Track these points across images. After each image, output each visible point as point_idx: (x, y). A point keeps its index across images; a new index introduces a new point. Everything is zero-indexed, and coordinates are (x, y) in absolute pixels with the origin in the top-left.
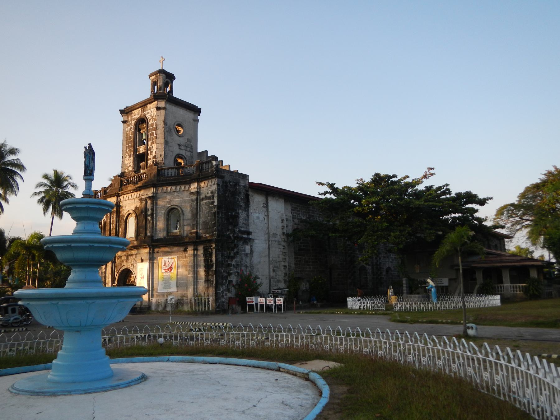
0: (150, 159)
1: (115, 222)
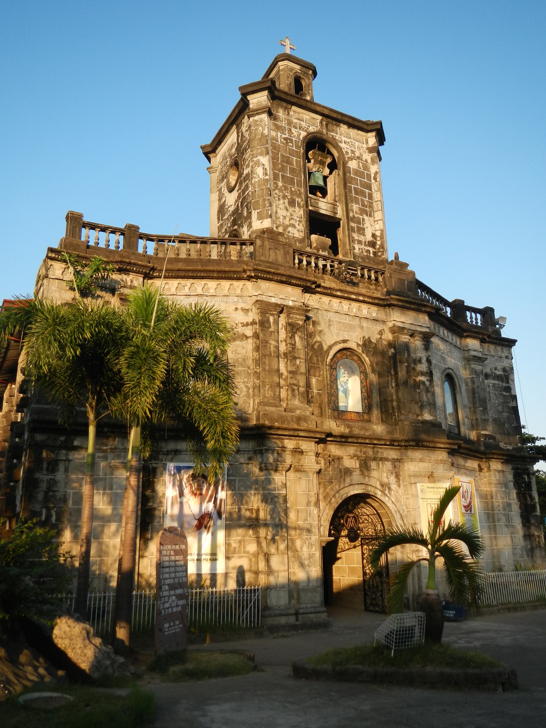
0: (360, 242)
1: (302, 356)
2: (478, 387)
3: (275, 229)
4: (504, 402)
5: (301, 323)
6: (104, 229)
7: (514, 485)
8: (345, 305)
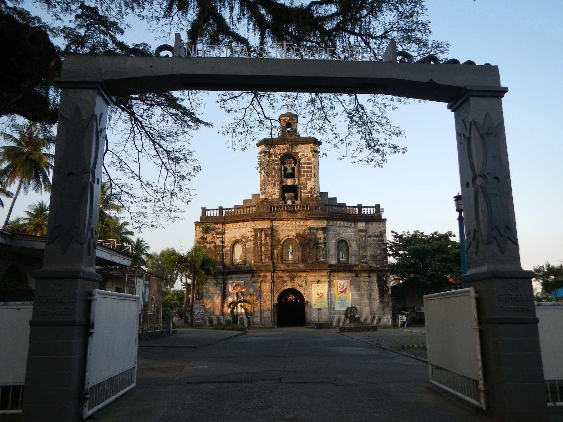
0: (304, 193)
1: (270, 244)
2: (362, 242)
3: (268, 197)
4: (379, 247)
5: (269, 233)
6: (212, 210)
7: (377, 282)
8: (289, 223)
